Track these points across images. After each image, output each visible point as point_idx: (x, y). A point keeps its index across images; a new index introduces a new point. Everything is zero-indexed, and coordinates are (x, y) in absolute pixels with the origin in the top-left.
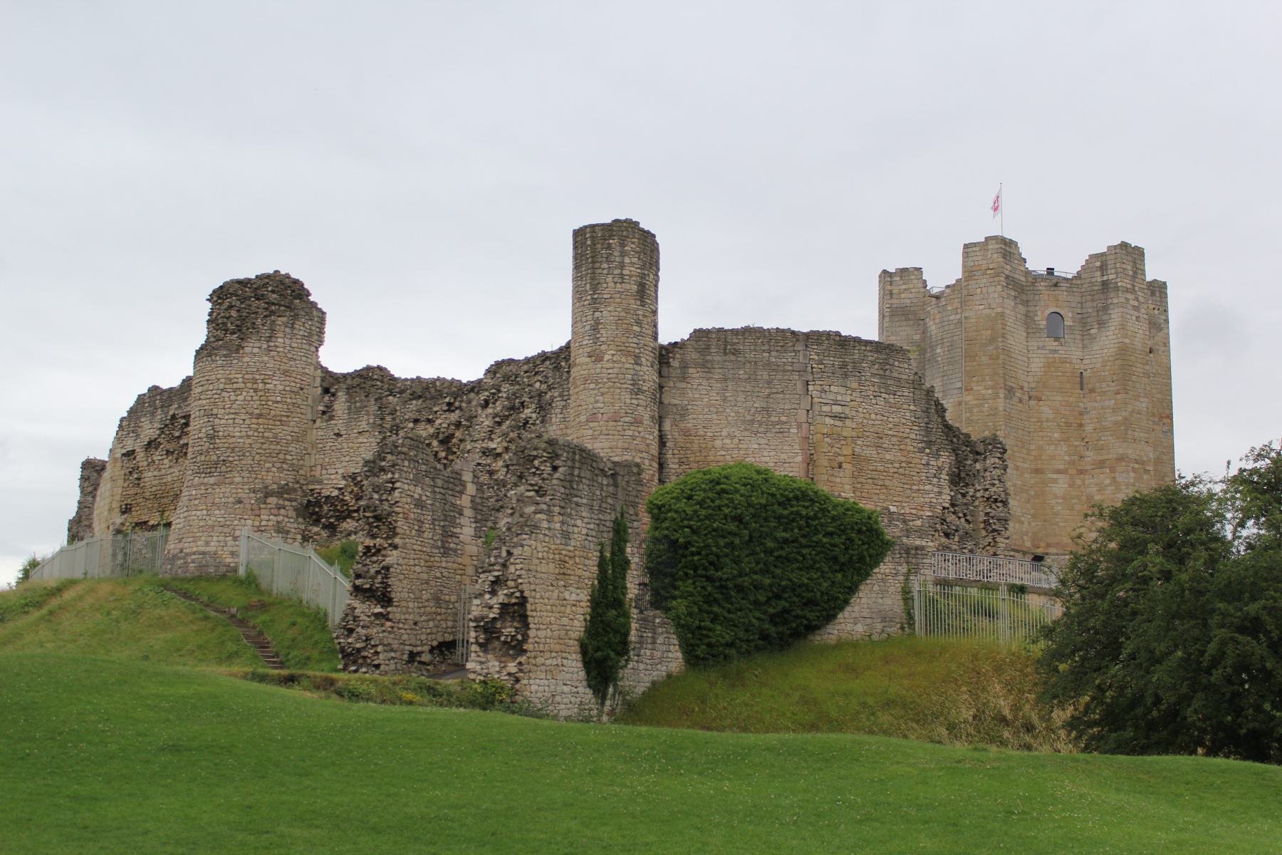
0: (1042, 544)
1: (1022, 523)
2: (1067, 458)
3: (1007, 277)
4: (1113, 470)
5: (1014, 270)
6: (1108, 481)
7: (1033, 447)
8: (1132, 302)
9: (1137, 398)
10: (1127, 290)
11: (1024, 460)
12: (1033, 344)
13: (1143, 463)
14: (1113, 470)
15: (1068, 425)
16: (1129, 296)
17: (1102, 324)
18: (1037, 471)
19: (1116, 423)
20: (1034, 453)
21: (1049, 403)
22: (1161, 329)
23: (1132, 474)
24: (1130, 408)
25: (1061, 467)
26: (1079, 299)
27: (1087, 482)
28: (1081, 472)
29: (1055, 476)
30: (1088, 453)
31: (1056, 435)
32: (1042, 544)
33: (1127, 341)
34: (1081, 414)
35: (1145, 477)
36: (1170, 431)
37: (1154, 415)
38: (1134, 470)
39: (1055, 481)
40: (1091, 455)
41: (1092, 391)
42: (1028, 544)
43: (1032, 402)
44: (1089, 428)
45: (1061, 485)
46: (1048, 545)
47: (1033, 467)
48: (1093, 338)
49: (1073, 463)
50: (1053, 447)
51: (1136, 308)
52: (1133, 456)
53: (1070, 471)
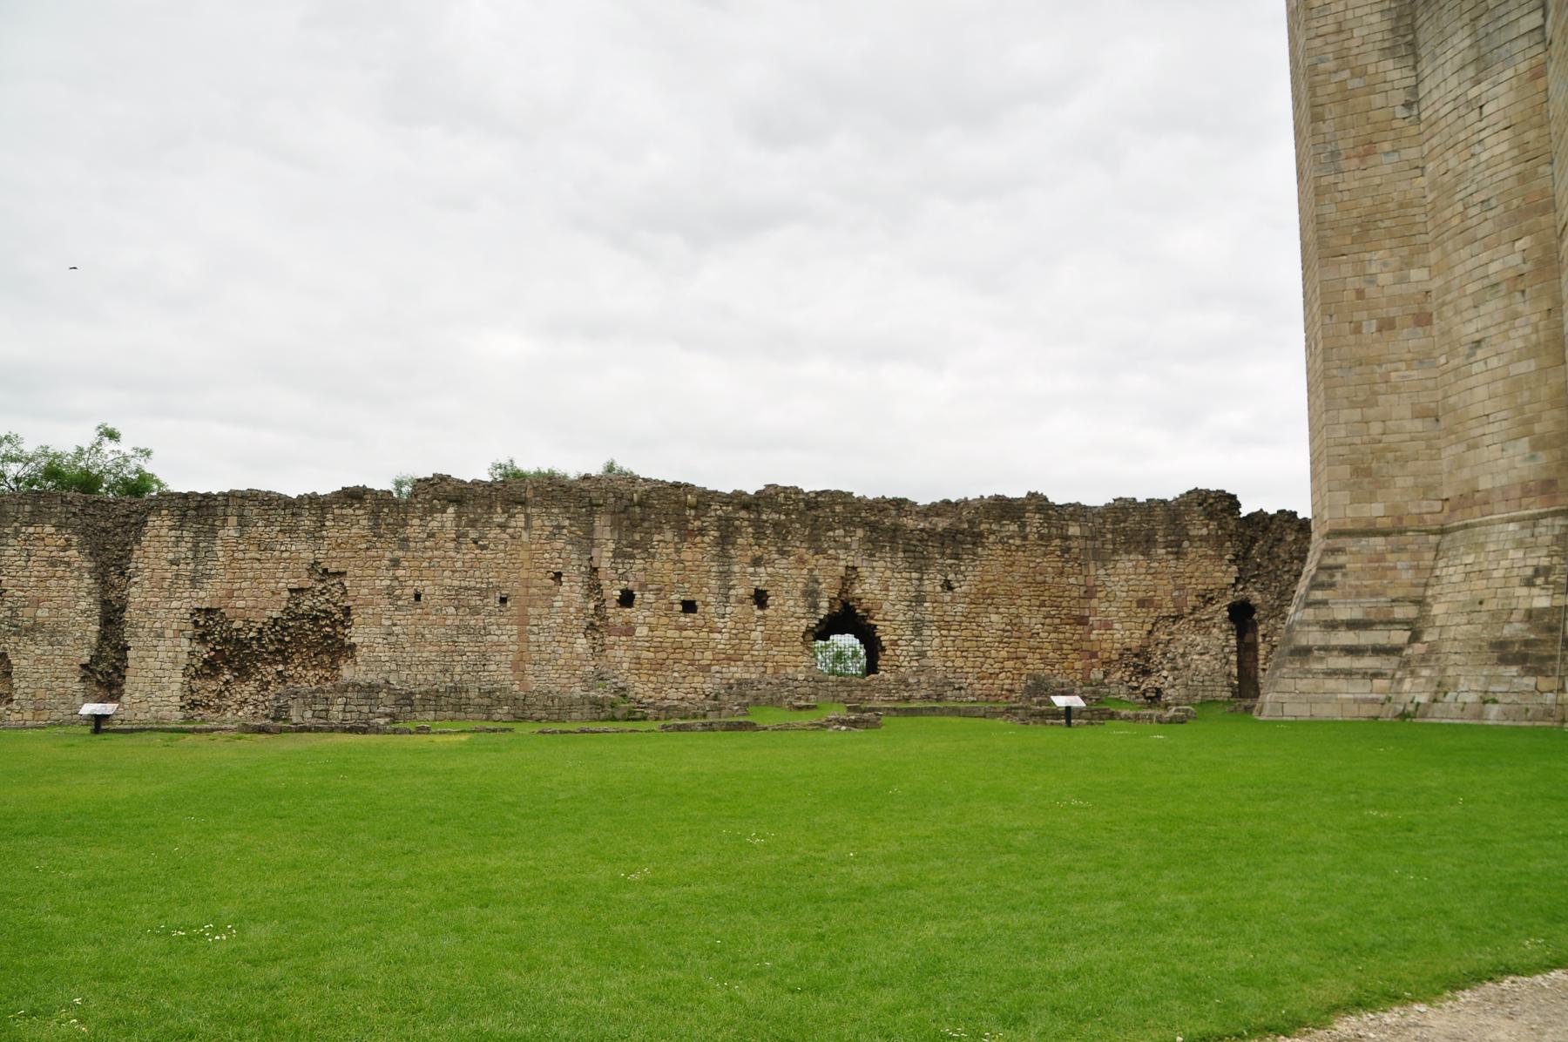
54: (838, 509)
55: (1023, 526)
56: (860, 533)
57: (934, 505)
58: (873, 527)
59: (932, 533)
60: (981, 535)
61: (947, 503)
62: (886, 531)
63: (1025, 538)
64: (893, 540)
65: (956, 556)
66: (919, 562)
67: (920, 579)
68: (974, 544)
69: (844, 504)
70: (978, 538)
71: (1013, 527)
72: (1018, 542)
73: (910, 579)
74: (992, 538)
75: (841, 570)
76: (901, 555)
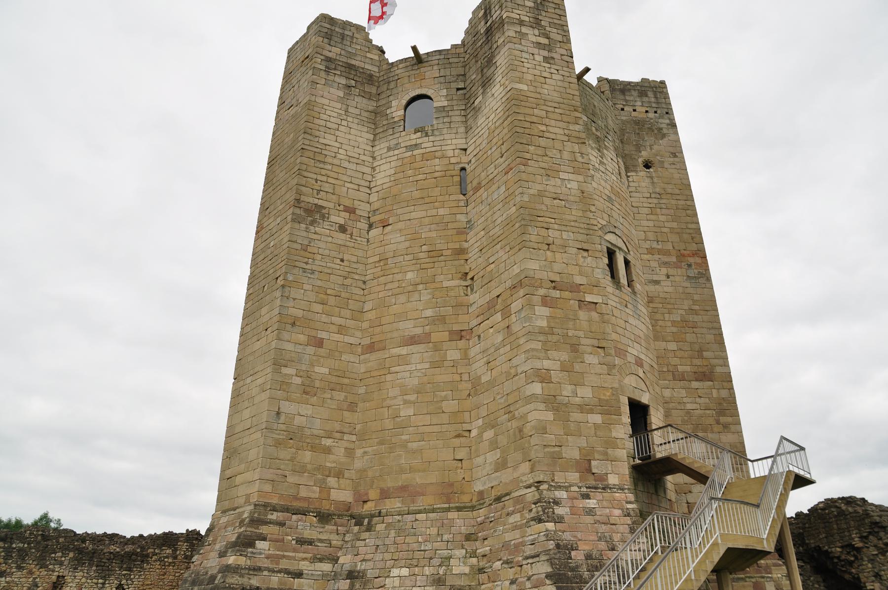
0: (373, 494)
1: (328, 450)
2: (429, 313)
3: (328, 60)
4: (506, 315)
5: (351, 55)
6: (500, 338)
7: (368, 306)
8: (534, 39)
9: (550, 172)
10: (521, 23)
11: (342, 330)
12: (381, 147)
13: (575, 288)
14: (506, 315)
15: (435, 254)
16: (524, 30)
17: (486, 83)
18: (371, 348)
19: (509, 223)
20: (371, 315)
21: (401, 225)
22: (664, 136)
23: (544, 311)
24: (535, 189)
25: (418, 331)
26: (461, 71)
27: (472, 353)
28: (460, 335)
29: (404, 351)
30: (472, 298)
31: (410, 275)
32: (373, 494)
33: (525, 87)
34: (462, 232)
35: (582, 315)
36: (702, 276)
37: (667, 253)
38: (545, 301)
39: (403, 360)
40: (478, 299)
41: (477, 189)
42: (342, 495)
43: (373, 233)
44: (473, 254)
45: (414, 366)
46: (385, 494)
47: (367, 341)
48: (477, 110)
49: (442, 319)
50: (403, 298)
51: (539, 45)
52: (544, 275)
53: (435, 337)
54: (61, 540)
55: (176, 550)
56: (71, 555)
57: (133, 537)
58: (80, 551)
59: (116, 555)
60: (147, 556)
61: (141, 536)
62: (88, 553)
63: (175, 558)
64: (91, 559)
65: (130, 569)
66: (104, 573)
67: (104, 584)
68: (142, 561)
69: (65, 537)
70: (145, 558)
71: (169, 551)
72: (170, 560)
73: (97, 584)
74: (155, 558)
75: (54, 578)
76: (94, 568)
